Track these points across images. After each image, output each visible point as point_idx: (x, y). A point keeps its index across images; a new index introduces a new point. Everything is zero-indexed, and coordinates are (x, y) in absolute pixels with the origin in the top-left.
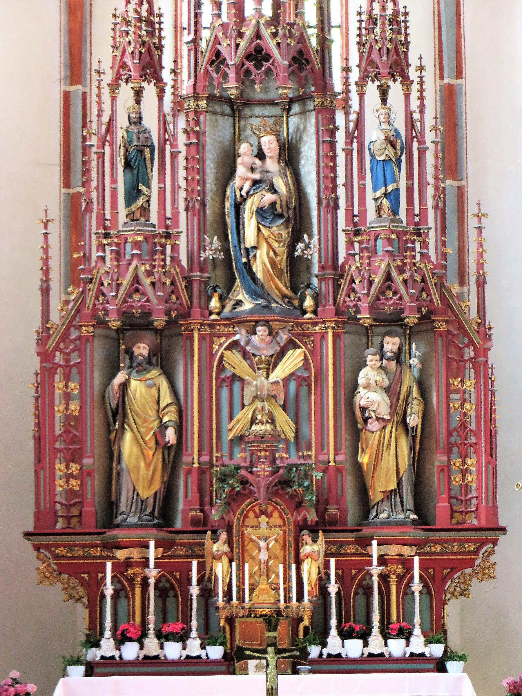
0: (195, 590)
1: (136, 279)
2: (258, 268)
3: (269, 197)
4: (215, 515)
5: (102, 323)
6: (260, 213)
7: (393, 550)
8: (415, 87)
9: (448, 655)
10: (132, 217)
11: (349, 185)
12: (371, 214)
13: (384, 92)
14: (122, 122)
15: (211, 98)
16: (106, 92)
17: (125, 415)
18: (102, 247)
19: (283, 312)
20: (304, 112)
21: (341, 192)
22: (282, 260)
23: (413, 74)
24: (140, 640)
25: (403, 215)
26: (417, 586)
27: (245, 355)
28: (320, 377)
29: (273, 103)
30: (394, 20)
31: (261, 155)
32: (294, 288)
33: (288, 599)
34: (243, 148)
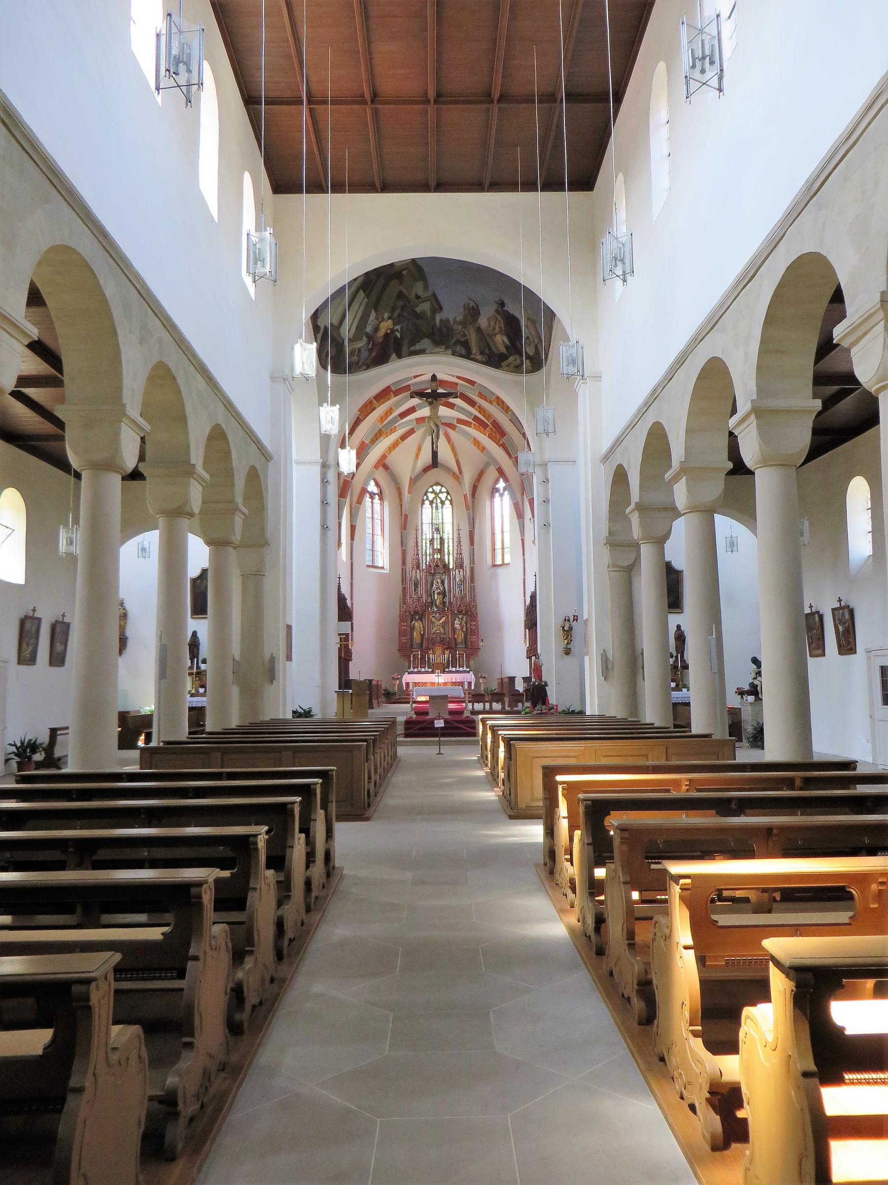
0: (427, 660)
1: (416, 605)
2: (437, 603)
3: (439, 591)
4: (430, 647)
5: (410, 613)
6: (438, 593)
7: (461, 652)
8: (465, 571)
9: (470, 670)
10: (415, 594)
11: (453, 588)
12: (457, 594)
13: (459, 572)
14: (413, 578)
15: (429, 573)
16: (410, 572)
17: (414, 629)
18: (410, 600)
19: (442, 611)
20: (445, 575)
21: (452, 589)
22: (442, 602)
23: (464, 568)
24: (417, 668)
25: (463, 593)
26: (465, 659)
27: (435, 618)
28: (448, 622)
29: (440, 573)
30: (461, 559)
31: (438, 583)
32: (443, 606)
33: (443, 661)
34: (435, 582)
